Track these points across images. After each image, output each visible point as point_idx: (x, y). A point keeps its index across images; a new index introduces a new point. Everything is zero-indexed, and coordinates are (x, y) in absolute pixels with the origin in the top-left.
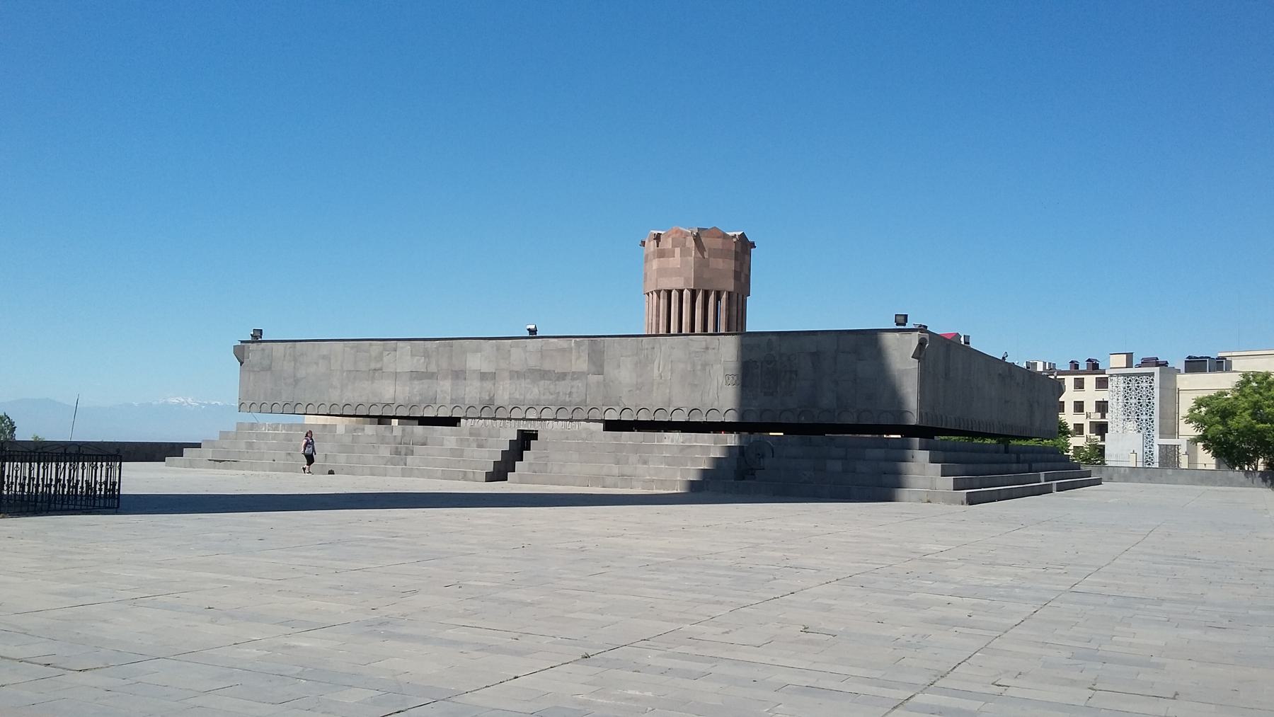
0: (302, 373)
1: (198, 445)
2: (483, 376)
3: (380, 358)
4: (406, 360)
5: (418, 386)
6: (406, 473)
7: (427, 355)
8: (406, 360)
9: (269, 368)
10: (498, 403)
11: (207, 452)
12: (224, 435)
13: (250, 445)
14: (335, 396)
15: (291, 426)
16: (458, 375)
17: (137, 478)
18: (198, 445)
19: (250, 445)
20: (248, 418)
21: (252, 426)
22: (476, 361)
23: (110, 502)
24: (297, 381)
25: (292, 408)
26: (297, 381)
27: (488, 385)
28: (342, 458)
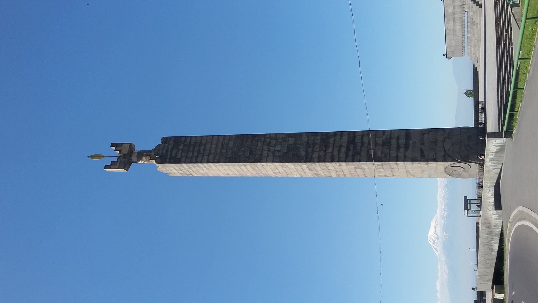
0: (454, 45)
1: (474, 65)
2: (454, 8)
3: (450, 30)
4: (450, 25)
5: (457, 21)
6: (480, 24)
7: (449, 20)
8: (450, 25)
9: (453, 52)
10: (461, 10)
11: (475, 63)
12: (471, 59)
13: (474, 54)
14: (460, 38)
15: (468, 46)
16: (454, 13)
17: (481, 99)
18: (474, 65)
19: (474, 54)
20: (466, 53)
21: (468, 53)
22: (450, 10)
23: (485, 101)
24: (456, 45)
25: (463, 46)
26: (456, 45)
27: (456, 7)
28: (476, 36)
